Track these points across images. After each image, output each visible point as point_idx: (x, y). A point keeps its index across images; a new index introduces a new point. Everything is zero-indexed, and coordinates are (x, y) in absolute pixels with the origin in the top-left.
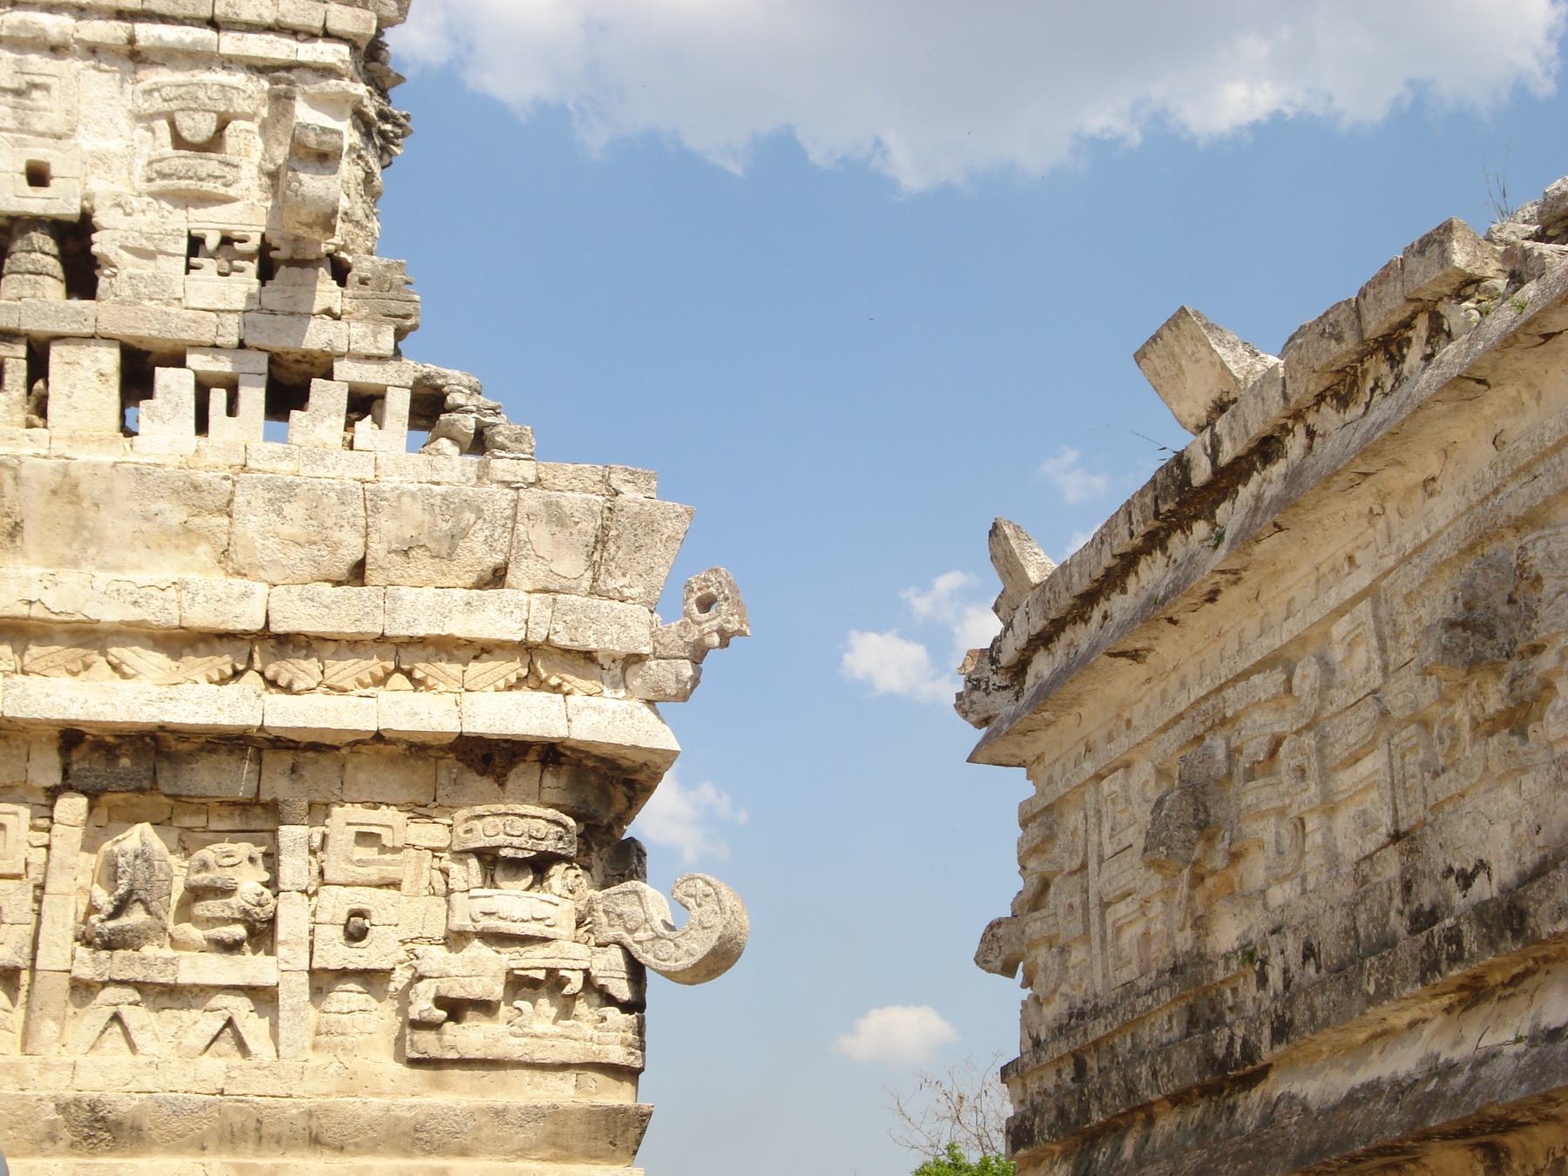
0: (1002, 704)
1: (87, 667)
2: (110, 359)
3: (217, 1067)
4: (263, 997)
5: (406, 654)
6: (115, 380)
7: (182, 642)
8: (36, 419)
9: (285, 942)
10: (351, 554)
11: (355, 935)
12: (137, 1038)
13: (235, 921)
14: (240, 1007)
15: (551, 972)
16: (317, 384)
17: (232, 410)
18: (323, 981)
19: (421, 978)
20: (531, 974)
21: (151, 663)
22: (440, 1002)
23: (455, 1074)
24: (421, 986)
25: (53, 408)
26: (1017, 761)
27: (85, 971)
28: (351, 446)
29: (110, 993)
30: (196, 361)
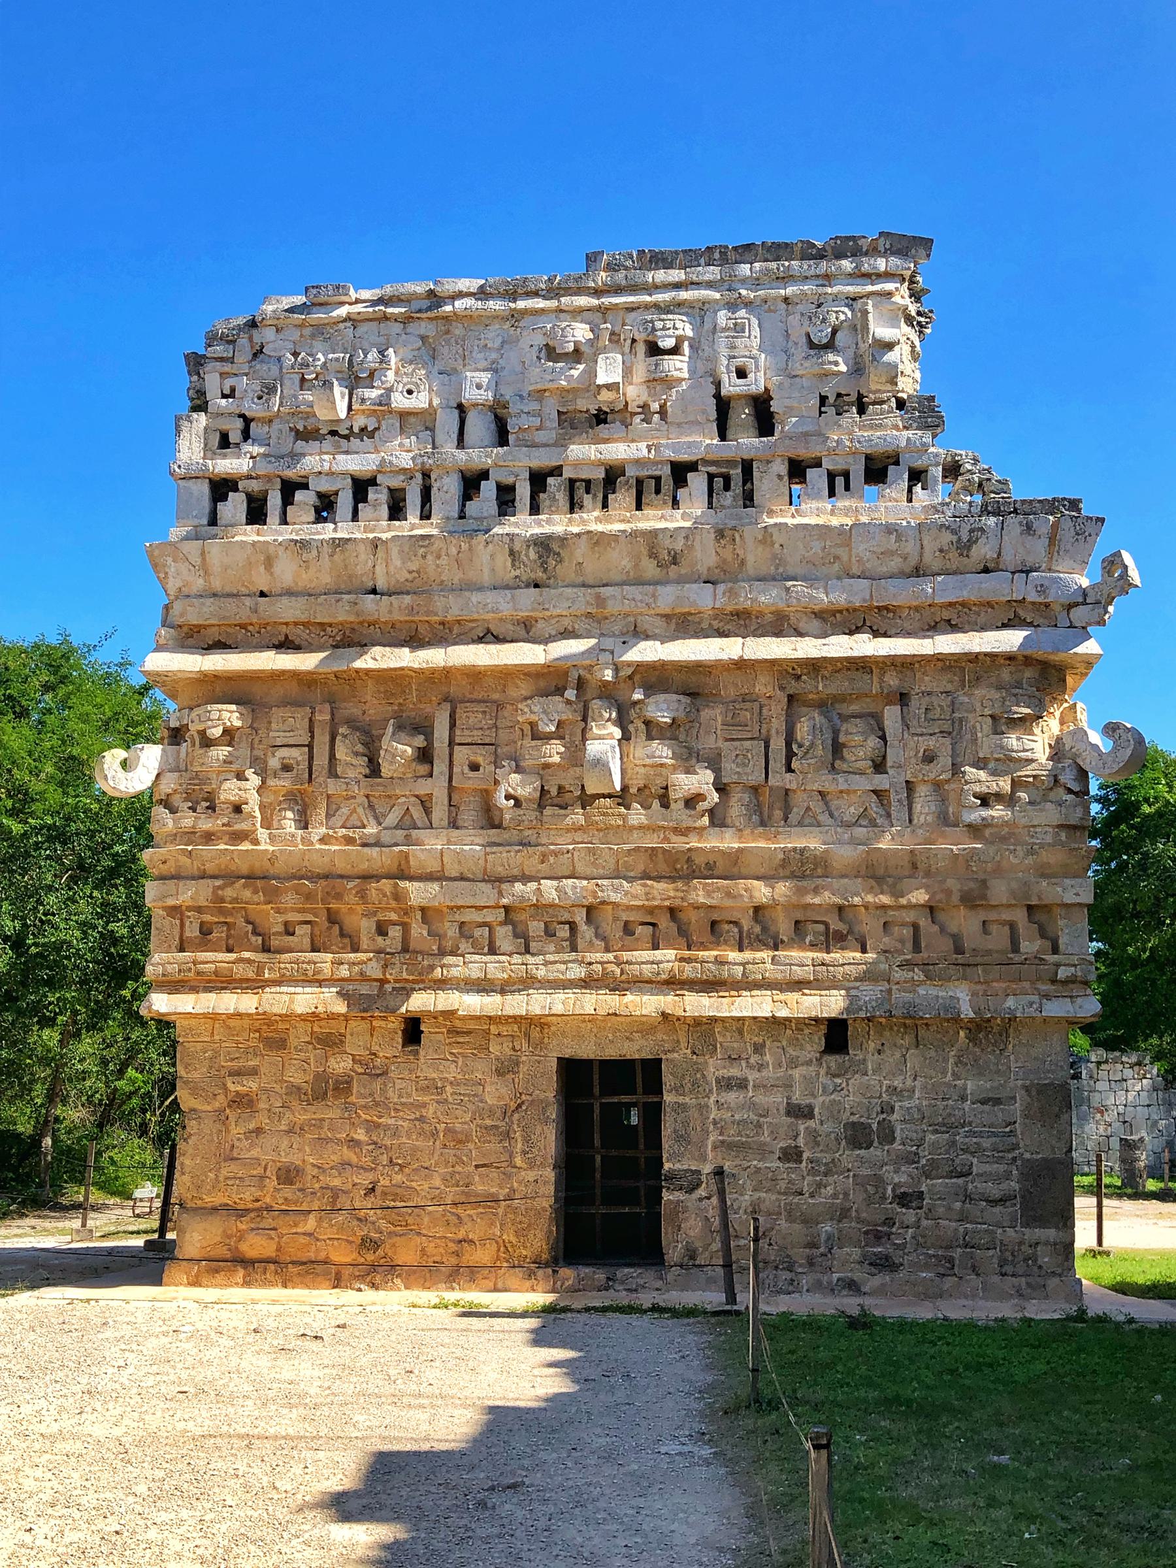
8: (748, 503)
10: (913, 562)
16: (891, 468)
17: (847, 488)
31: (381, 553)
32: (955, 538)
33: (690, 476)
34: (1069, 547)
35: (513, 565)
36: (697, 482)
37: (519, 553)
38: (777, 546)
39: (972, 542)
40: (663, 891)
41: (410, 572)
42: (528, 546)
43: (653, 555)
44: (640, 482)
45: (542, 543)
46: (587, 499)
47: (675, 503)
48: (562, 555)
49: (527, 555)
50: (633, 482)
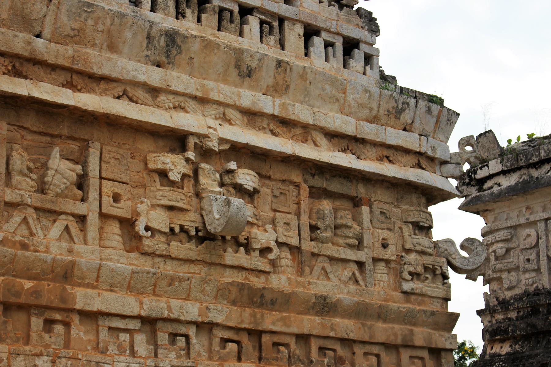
0: (474, 192)
1: (307, 141)
2: (299, 29)
3: (352, 287)
4: (360, 265)
5: (390, 152)
6: (303, 38)
7: (334, 136)
9: (366, 247)
10: (374, 113)
11: (385, 246)
12: (331, 276)
13: (353, 238)
14: (355, 267)
15: (433, 265)
18: (375, 260)
19: (405, 264)
20: (429, 266)
21: (323, 141)
22: (411, 273)
23: (413, 297)
24: (406, 266)
25: (287, 45)
26: (476, 211)
27: (316, 251)
28: (364, 74)
29: (320, 259)
30: (323, 34)
31: (52, 7)
32: (395, 105)
33: (250, 17)
34: (443, 127)
35: (147, 46)
36: (253, 22)
37: (154, 38)
38: (308, 82)
39: (403, 110)
40: (243, 317)
41: (73, 30)
42: (161, 35)
43: (237, 66)
44: (222, 10)
45: (171, 35)
46: (188, 12)
47: (241, 35)
48: (183, 48)
49: (159, 42)
50: (217, 9)
